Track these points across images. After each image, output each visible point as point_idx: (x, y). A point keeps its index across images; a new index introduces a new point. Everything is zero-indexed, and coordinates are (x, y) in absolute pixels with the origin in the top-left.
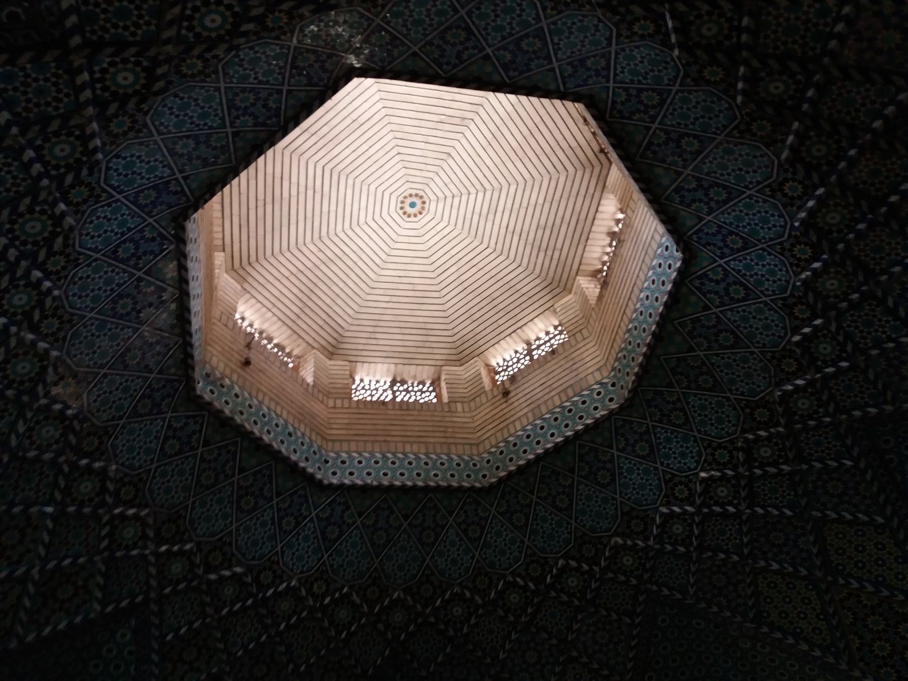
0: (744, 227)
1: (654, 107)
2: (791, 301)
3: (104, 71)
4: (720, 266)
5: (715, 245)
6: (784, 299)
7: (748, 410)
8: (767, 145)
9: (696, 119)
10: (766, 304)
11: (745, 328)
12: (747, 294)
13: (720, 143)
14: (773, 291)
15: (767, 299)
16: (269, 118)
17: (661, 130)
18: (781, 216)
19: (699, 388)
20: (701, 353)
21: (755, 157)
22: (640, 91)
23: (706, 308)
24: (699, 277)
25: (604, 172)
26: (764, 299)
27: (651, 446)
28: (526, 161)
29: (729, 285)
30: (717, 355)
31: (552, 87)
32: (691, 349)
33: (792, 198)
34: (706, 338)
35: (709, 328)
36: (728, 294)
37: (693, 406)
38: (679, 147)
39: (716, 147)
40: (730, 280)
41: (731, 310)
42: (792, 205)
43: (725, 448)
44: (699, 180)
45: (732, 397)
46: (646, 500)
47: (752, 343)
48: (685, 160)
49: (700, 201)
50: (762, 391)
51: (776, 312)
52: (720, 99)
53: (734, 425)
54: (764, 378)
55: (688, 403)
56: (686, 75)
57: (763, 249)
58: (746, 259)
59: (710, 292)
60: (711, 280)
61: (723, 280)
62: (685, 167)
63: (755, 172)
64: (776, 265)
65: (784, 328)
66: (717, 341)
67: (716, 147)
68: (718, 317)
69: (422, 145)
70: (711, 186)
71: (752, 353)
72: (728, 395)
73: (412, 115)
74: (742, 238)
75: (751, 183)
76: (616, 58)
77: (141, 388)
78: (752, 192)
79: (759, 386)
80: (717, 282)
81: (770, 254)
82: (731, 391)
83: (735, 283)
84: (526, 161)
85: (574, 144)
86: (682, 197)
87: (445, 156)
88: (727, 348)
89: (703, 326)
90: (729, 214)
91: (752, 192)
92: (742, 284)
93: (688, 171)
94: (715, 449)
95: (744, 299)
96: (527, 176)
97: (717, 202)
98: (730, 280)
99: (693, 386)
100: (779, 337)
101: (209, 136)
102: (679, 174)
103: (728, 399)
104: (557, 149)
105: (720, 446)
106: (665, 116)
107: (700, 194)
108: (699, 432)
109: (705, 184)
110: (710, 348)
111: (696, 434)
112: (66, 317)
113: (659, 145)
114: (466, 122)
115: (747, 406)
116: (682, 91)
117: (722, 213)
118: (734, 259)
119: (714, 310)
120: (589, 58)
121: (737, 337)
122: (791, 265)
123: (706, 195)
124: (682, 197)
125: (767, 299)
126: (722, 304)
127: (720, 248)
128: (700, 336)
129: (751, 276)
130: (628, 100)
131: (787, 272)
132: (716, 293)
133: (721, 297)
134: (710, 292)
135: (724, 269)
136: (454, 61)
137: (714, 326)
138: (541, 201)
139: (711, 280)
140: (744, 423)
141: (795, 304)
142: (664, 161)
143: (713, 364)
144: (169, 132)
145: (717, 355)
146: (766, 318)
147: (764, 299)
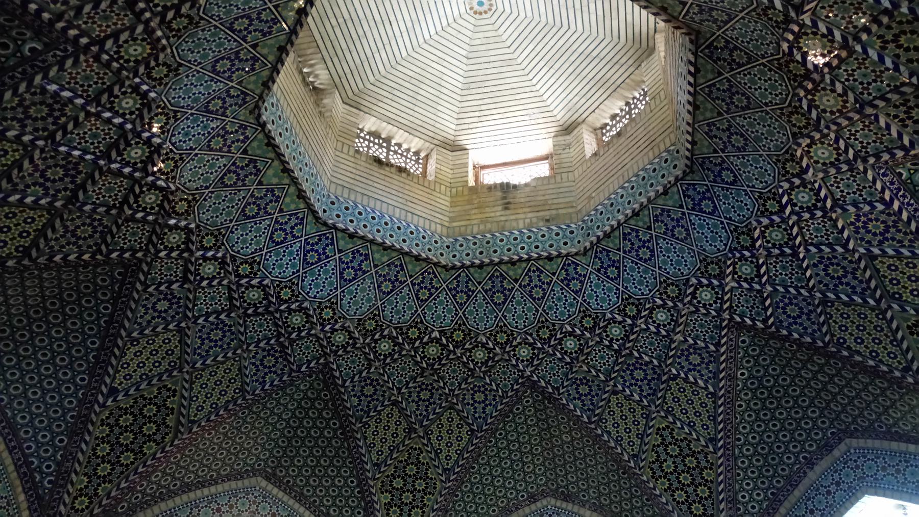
0: (319, 271)
1: (418, 291)
2: (256, 267)
3: (715, 302)
4: (302, 236)
5: (317, 243)
6: (259, 263)
7: (190, 198)
8: (359, 320)
9: (397, 302)
10: (261, 250)
11: (252, 227)
12: (274, 242)
13: (376, 301)
14: (268, 260)
15: (264, 252)
16: (629, 234)
17: (405, 281)
18: (315, 297)
19: (229, 171)
20: (252, 188)
21: (357, 309)
22: (431, 294)
23: (281, 211)
24: (302, 219)
25: (344, 95)
26: (265, 251)
27: (212, 112)
28: (408, 79)
29: (287, 234)
30: (244, 198)
31: (472, 270)
32: (260, 183)
33: (322, 310)
34: (261, 198)
35: (267, 204)
36: (281, 229)
37: (218, 159)
38: (390, 280)
39: (375, 297)
40: (289, 237)
41: (269, 225)
42: (318, 307)
43: (172, 171)
44: (364, 272)
45: (207, 191)
46: (175, 90)
47: (238, 225)
48: (380, 276)
49: (351, 261)
50: (199, 213)
51: (252, 253)
52: (399, 323)
53: (185, 183)
54: (208, 220)
55: (222, 157)
56: (422, 322)
57: (298, 271)
58: (297, 255)
59: (290, 219)
60: (296, 225)
61: (292, 232)
62: (377, 272)
63: (349, 303)
64: (284, 272)
65: (238, 252)
66: (254, 203)
67: (375, 297)
68: (270, 214)
69: (492, 59)
70: (356, 275)
71: (231, 221)
72: (210, 190)
73: (508, 81)
74: (312, 264)
75: (344, 296)
76: (455, 307)
77: (739, 73)
78: (338, 292)
79: (204, 213)
80: (292, 228)
81: (294, 274)
82: (212, 192)
83: (285, 238)
84: (408, 79)
85: (380, 104)
86: (361, 255)
87: (471, 55)
88: (245, 207)
89: (271, 201)
90: (333, 269)
91: (338, 292)
92: (282, 242)
93: (373, 271)
94: (176, 162)
95: (271, 238)
96: (399, 68)
97: (344, 269)
98: (289, 237)
99: (233, 168)
100: (233, 246)
101: (665, 233)
102: (376, 266)
103: (207, 188)
104: (390, 96)
105: (176, 167)
106: (410, 290)
107: (355, 264)
108: (196, 155)
109: (359, 273)
110: (252, 196)
111: (196, 151)
112: (780, 165)
113: (398, 272)
114: (466, 86)
115: (194, 199)
116: (416, 312)
117: (335, 266)
118: (300, 248)
119: (276, 214)
120: (467, 300)
121: (249, 218)
122: (281, 282)
123: (353, 268)
124: (361, 255)
125: (264, 252)
126: (277, 222)
127: (313, 245)
128: (266, 195)
129: (284, 252)
130: (431, 283)
131: (277, 277)
132: (286, 223)
133: (282, 224)
134: (290, 219)
135: (298, 237)
136: (531, 274)
137: (265, 208)
138: (377, 55)
139: (296, 225)
140: (183, 191)
141: (252, 268)
142: (388, 265)
143: (239, 191)
144: (689, 249)
145: (244, 198)
146: (251, 244)
147: (265, 251)
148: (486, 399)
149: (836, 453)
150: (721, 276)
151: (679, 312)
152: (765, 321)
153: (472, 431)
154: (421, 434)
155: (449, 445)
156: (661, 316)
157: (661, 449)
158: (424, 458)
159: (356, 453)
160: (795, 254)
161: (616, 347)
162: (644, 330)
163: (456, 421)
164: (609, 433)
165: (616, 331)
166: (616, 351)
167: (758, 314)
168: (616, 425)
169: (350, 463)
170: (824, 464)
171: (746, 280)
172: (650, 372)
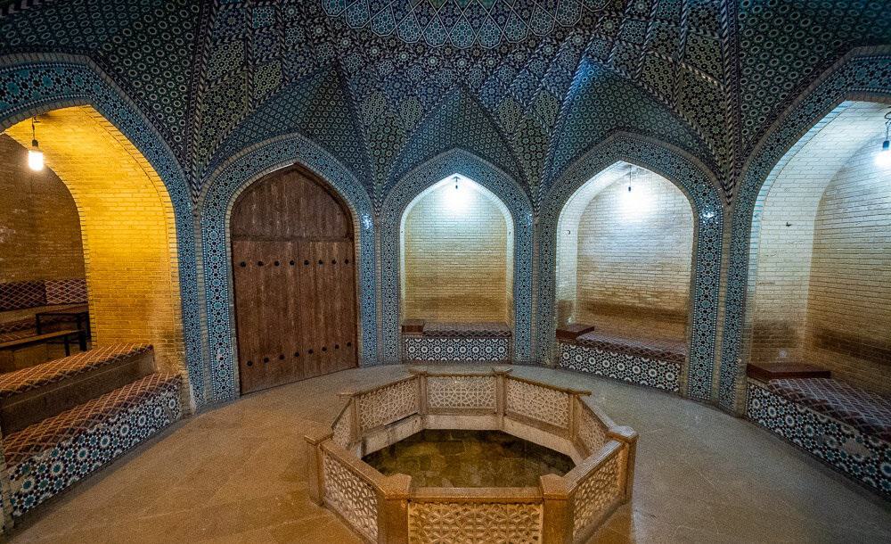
148: (304, 62)
149: (449, 152)
150: (476, 59)
151: (443, 64)
152: (477, 90)
153: (284, 80)
154: (251, 70)
155: (264, 83)
156: (433, 61)
157: (381, 128)
158: (244, 87)
159: (197, 67)
160: (518, 70)
161: (398, 66)
162: (419, 64)
163: (278, 69)
164: (361, 110)
165: (404, 56)
166: (396, 68)
167: (477, 85)
168: (367, 107)
169: (188, 73)
170: (442, 155)
171: (486, 67)
172: (404, 86)
